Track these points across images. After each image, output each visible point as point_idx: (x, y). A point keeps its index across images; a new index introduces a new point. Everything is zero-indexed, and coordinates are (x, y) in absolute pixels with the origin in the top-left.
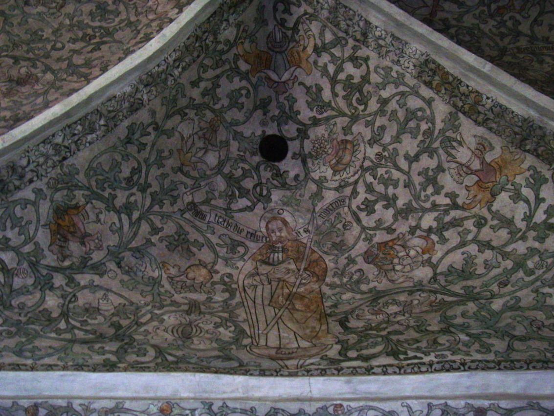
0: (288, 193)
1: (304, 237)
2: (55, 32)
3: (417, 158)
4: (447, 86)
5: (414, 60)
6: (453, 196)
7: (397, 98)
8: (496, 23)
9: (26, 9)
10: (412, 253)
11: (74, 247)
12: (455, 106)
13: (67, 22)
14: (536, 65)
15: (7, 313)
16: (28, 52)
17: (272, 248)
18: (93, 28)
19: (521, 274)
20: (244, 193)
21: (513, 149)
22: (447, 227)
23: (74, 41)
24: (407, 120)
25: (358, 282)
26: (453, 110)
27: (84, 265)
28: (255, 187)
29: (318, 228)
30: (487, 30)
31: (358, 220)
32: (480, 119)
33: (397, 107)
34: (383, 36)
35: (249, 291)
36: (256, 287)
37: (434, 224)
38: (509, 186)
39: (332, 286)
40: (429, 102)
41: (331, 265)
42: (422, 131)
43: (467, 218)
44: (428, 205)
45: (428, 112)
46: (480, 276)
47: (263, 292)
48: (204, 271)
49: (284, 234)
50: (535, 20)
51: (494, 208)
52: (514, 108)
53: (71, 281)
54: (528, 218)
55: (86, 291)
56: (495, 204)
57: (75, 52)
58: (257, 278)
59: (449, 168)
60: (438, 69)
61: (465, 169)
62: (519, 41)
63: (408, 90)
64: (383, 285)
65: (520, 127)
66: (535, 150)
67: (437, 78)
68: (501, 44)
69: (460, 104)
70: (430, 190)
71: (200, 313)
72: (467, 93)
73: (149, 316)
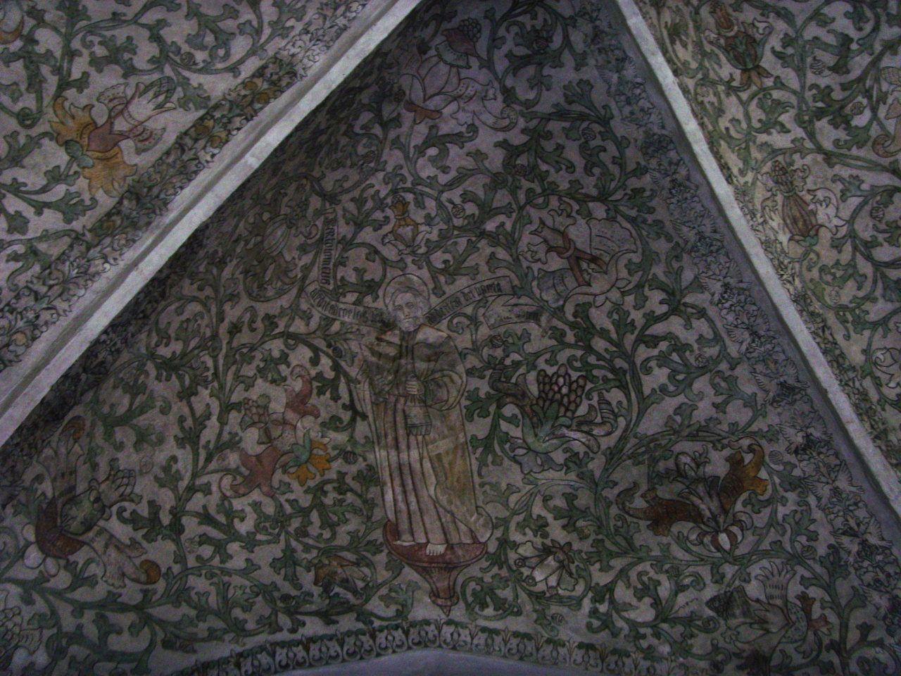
3: (156, 38)
4: (249, 99)
5: (300, 56)
6: (82, 84)
7: (255, 23)
8: (382, 195)
12: (217, 106)
14: (298, 241)
21: (129, 180)
22: (32, 68)
24: (217, 32)
26: (212, 103)
30: (372, 181)
32: (188, 141)
33: (242, 20)
34: (348, 14)
37: (40, 49)
38: (75, 168)
40: (234, 70)
42: (192, 51)
43: (40, 99)
44: (76, 44)
45: (220, 66)
50: (377, 252)
51: (46, 141)
52: (187, 191)
54: (16, 189)
56: (53, 144)
59: (127, 85)
60: (277, 88)
61: (120, 107)
62: (347, 224)
63: (262, 41)
65: (157, 197)
66: (119, 213)
67: (266, 86)
68: (345, 198)
69: (217, 115)
70: (100, 51)
72: (230, 127)
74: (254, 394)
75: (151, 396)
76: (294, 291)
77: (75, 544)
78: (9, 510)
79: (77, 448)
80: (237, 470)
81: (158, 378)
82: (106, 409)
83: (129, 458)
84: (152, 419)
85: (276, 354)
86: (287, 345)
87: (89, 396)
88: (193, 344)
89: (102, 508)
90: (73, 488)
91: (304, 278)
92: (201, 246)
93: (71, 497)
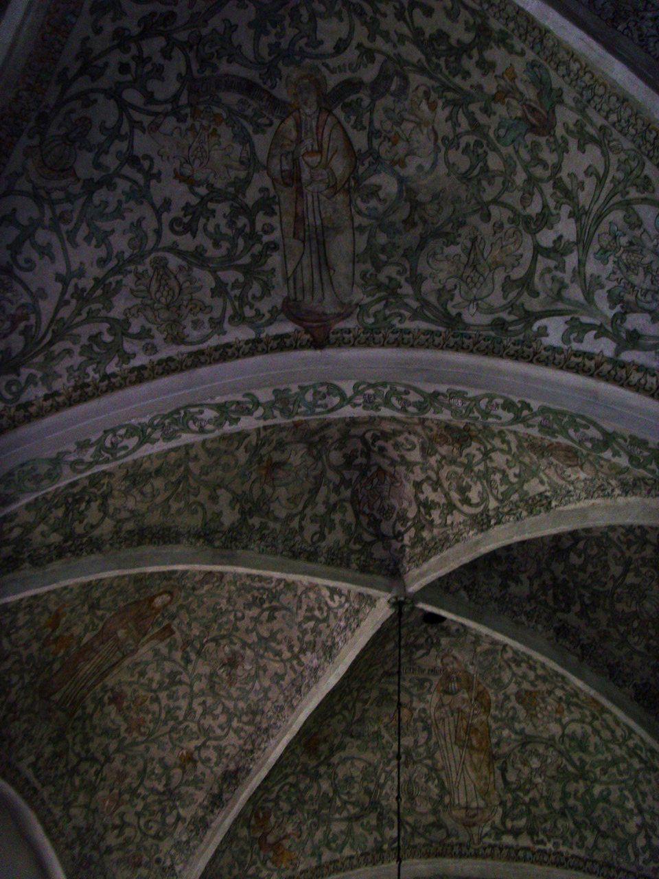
0: (453, 639)
1: (471, 669)
2: (229, 600)
9: (197, 592)
10: (549, 708)
11: (324, 748)
13: (233, 588)
15: (306, 807)
16: (219, 629)
17: (448, 678)
18: (258, 589)
19: (614, 770)
20: (419, 647)
23: (249, 606)
25: (513, 718)
27: (332, 752)
28: (427, 640)
29: (480, 663)
31: (510, 666)
35: (440, 726)
41: (493, 698)
47: (448, 727)
49: (456, 666)
53: (329, 765)
55: (340, 767)
57: (256, 620)
58: (443, 710)
64: (529, 730)
68: (628, 554)
71: (415, 763)
73: (383, 776)
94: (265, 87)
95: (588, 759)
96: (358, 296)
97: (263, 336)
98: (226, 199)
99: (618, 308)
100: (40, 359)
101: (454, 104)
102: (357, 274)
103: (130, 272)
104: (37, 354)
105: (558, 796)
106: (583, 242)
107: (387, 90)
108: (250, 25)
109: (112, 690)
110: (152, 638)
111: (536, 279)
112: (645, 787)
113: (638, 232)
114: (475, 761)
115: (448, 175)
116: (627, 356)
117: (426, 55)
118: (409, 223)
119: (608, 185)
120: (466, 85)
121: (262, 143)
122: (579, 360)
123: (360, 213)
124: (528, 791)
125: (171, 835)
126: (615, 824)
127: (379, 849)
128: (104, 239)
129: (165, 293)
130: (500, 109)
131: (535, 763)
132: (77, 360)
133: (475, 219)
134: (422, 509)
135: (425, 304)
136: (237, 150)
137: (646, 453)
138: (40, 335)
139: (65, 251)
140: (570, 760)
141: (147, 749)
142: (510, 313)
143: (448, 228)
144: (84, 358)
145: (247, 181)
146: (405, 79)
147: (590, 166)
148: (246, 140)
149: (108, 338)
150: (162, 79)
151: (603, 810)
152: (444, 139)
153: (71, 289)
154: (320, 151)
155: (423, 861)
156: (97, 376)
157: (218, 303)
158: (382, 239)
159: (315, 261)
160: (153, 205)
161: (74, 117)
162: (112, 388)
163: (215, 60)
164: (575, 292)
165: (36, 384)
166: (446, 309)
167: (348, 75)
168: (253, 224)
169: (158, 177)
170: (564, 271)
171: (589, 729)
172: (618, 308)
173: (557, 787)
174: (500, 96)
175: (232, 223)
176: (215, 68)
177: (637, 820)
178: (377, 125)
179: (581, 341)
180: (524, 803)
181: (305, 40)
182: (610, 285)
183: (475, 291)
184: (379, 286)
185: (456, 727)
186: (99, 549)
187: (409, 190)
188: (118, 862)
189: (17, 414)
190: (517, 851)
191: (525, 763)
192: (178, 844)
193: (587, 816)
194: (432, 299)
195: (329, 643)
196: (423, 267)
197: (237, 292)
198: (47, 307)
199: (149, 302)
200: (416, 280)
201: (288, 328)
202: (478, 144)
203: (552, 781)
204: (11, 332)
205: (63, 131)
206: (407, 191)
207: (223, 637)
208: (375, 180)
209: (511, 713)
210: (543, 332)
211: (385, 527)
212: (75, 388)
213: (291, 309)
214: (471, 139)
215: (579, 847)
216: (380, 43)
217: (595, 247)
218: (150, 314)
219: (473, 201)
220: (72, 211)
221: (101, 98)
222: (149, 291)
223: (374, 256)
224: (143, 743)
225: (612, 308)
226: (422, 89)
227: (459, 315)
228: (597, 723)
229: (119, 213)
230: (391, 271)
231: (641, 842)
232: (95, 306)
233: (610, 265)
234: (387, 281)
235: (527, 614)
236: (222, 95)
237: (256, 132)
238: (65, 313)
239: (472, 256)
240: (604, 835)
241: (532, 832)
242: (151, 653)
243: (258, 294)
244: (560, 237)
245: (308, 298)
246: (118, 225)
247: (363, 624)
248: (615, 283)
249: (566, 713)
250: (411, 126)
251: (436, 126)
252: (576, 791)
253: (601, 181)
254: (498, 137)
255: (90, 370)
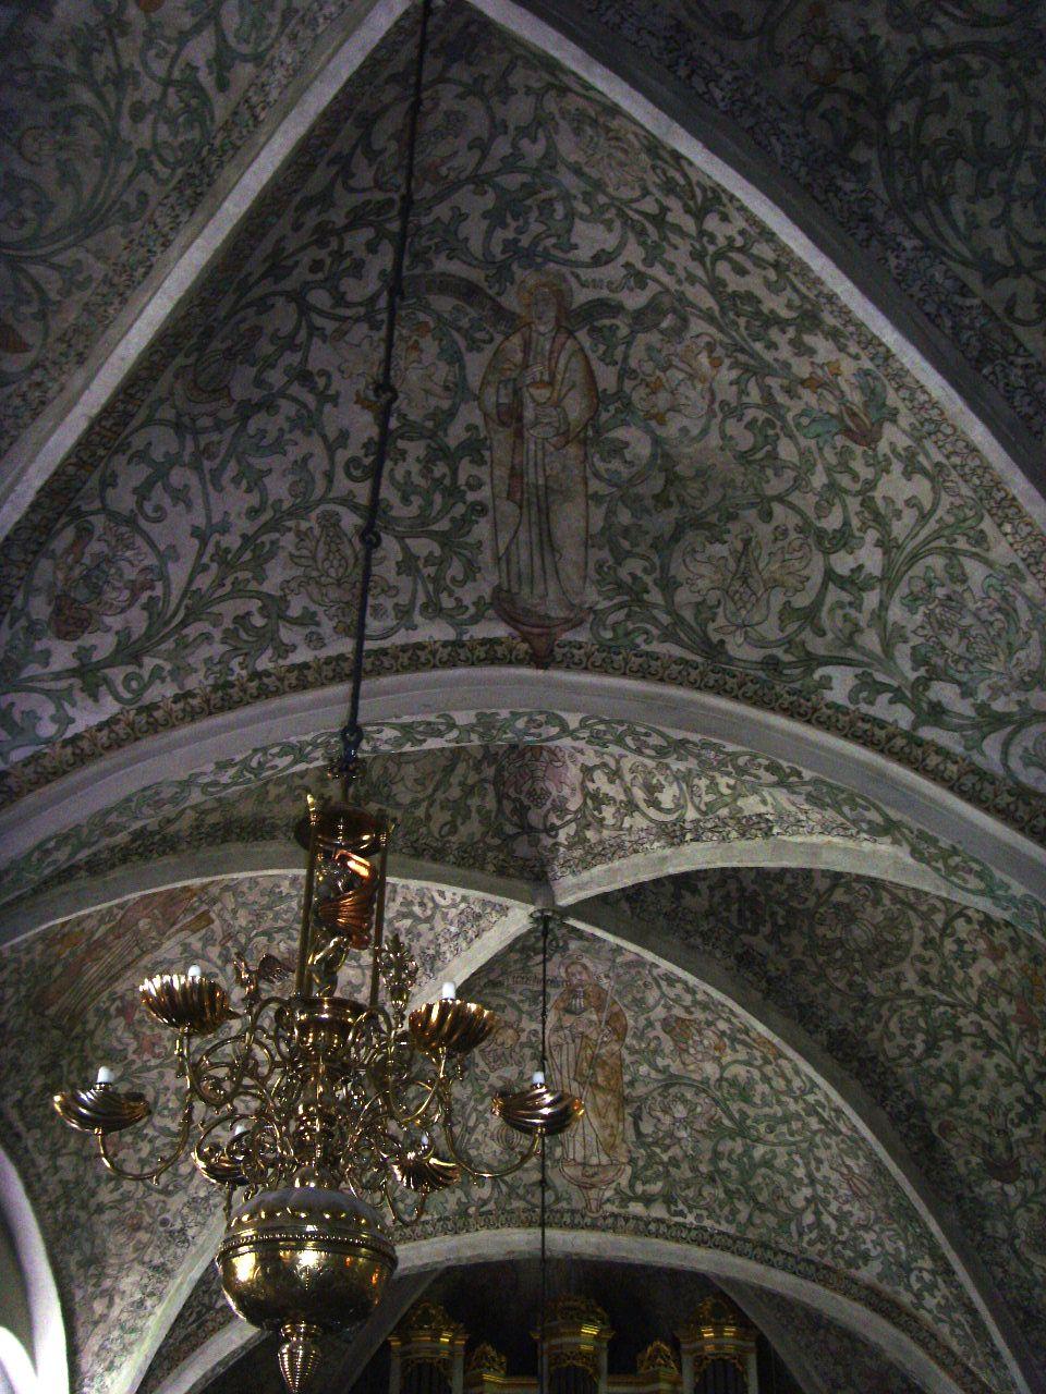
1: (605, 983)
10: (706, 1042)
16: (275, 919)
17: (573, 992)
19: (784, 1128)
29: (618, 976)
31: (659, 986)
36: (561, 1046)
39: (632, 1051)
41: (631, 1022)
46: (755, 1105)
48: (510, 1032)
49: (585, 977)
64: (675, 1067)
74: (978, 982)
75: (947, 1065)
76: (911, 913)
77: (1015, 1164)
78: (977, 1189)
79: (961, 1130)
80: (1023, 1031)
81: (937, 1057)
82: (944, 1103)
83: (983, 1096)
84: (964, 1069)
85: (954, 947)
86: (952, 935)
87: (928, 1115)
88: (923, 1024)
89: (1004, 1132)
90: (984, 1144)
91: (902, 902)
92: (843, 1031)
93: (989, 1148)
94: (491, 292)
95: (751, 1112)
96: (592, 596)
97: (466, 638)
98: (422, 437)
99: (922, 672)
100: (169, 645)
101: (746, 369)
102: (591, 565)
103: (290, 529)
104: (163, 640)
105: (708, 1155)
106: (889, 580)
107: (656, 325)
108: (485, 215)
109: (122, 998)
110: (182, 930)
111: (824, 613)
112: (821, 1153)
113: (959, 588)
114: (600, 1102)
115: (722, 449)
116: (928, 733)
117: (722, 308)
118: (662, 500)
119: (932, 525)
120: (768, 356)
121: (476, 365)
122: (867, 726)
123: (597, 475)
124: (669, 1147)
125: (185, 1189)
126: (777, 1195)
127: (464, 1213)
128: (256, 481)
129: (335, 563)
130: (808, 396)
131: (680, 1111)
132: (218, 649)
133: (751, 515)
134: (589, 802)
135: (679, 621)
136: (443, 372)
137: (932, 850)
138: (169, 613)
139: (206, 495)
140: (727, 1111)
141: (162, 1075)
142: (786, 651)
143: (713, 518)
144: (227, 648)
145: (452, 414)
146: (685, 321)
147: (914, 497)
148: (455, 359)
149: (258, 621)
150: (359, 277)
151: (764, 1177)
152: (723, 403)
153: (210, 549)
154: (551, 384)
155: (522, 1230)
156: (244, 673)
157: (405, 582)
158: (625, 517)
159: (535, 538)
160: (324, 437)
161: (244, 327)
162: (264, 693)
163: (430, 255)
164: (871, 640)
165: (163, 680)
166: (705, 632)
167: (605, 293)
168: (455, 473)
169: (334, 400)
170: (859, 609)
171: (756, 1075)
172: (922, 672)
173: (706, 1145)
174: (812, 383)
175: (426, 471)
176: (429, 264)
177: (807, 1192)
178: (633, 363)
179: (871, 703)
180: (662, 1163)
181: (553, 240)
182: (915, 641)
183: (744, 612)
184: (620, 586)
185: (577, 1056)
186: (173, 849)
187: (666, 456)
188: (111, 1224)
189: (138, 719)
190: (647, 1224)
191: (666, 1110)
192: (193, 1203)
193: (743, 1183)
194: (688, 615)
195: (431, 952)
196: (678, 570)
197: (431, 570)
198: (178, 574)
199: (315, 574)
200: (668, 585)
201: (500, 630)
202: (769, 423)
203: (699, 1137)
204: (130, 606)
205: (223, 346)
206: (663, 457)
207: (280, 930)
208: (620, 433)
209: (653, 1045)
210: (826, 683)
211: (534, 817)
212: (215, 688)
213: (503, 604)
214: (762, 415)
215: (728, 1222)
216: (658, 271)
217: (902, 590)
218: (313, 588)
219: (750, 491)
220: (219, 443)
221: (280, 302)
222: (314, 558)
223: (612, 539)
224: (157, 1067)
225: (915, 669)
226: (707, 339)
227: (722, 642)
228: (768, 1069)
229: (278, 447)
230: (634, 565)
231: (809, 1218)
232: (242, 575)
233: (919, 617)
234: (629, 580)
235: (702, 934)
236: (431, 298)
237: (470, 350)
238: (204, 582)
239: (743, 564)
240: (762, 1208)
241: (669, 1200)
242: (179, 949)
243: (460, 577)
244: (860, 567)
245: (526, 590)
246: (277, 462)
247: (486, 935)
248: (922, 640)
249: (728, 1051)
250: (681, 376)
251: (715, 385)
252: (732, 1152)
253: (924, 517)
254: (798, 425)
255: (235, 663)
